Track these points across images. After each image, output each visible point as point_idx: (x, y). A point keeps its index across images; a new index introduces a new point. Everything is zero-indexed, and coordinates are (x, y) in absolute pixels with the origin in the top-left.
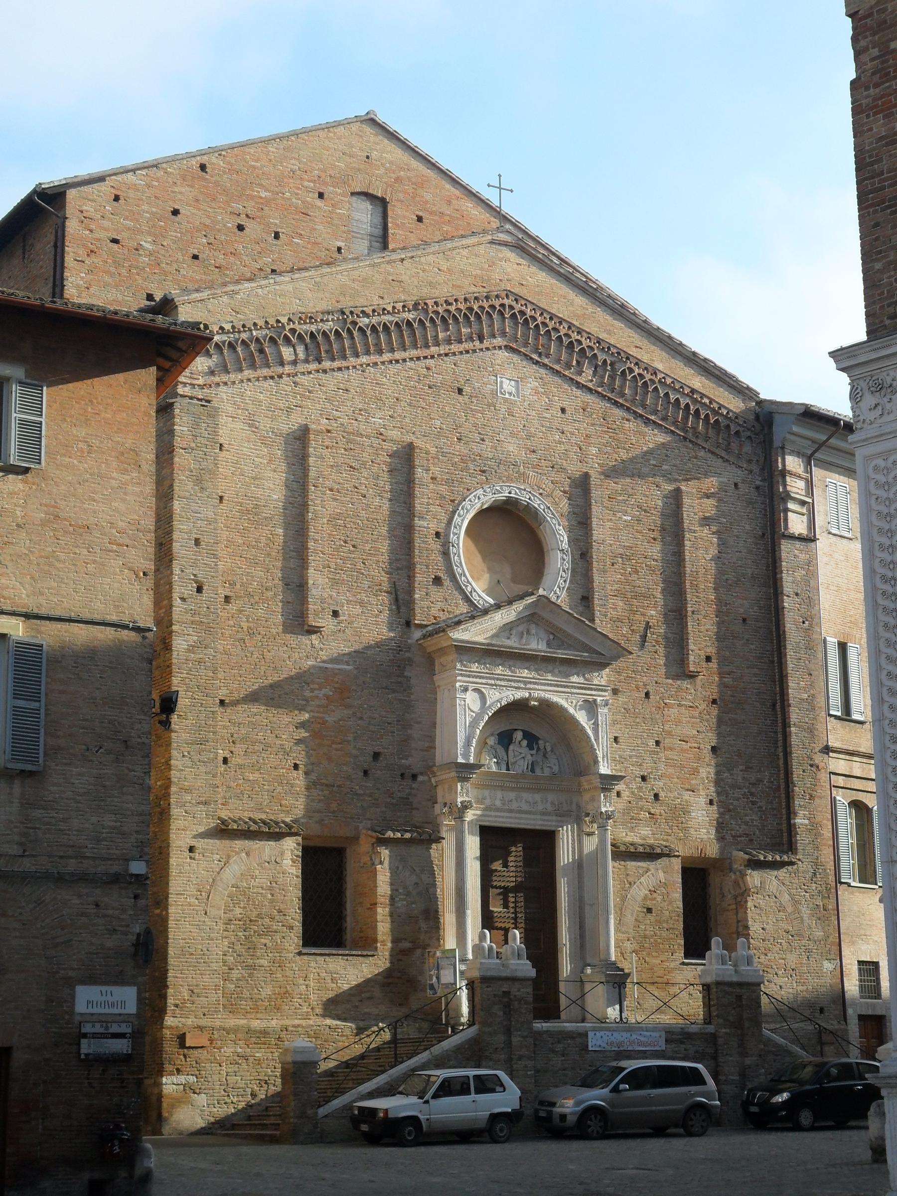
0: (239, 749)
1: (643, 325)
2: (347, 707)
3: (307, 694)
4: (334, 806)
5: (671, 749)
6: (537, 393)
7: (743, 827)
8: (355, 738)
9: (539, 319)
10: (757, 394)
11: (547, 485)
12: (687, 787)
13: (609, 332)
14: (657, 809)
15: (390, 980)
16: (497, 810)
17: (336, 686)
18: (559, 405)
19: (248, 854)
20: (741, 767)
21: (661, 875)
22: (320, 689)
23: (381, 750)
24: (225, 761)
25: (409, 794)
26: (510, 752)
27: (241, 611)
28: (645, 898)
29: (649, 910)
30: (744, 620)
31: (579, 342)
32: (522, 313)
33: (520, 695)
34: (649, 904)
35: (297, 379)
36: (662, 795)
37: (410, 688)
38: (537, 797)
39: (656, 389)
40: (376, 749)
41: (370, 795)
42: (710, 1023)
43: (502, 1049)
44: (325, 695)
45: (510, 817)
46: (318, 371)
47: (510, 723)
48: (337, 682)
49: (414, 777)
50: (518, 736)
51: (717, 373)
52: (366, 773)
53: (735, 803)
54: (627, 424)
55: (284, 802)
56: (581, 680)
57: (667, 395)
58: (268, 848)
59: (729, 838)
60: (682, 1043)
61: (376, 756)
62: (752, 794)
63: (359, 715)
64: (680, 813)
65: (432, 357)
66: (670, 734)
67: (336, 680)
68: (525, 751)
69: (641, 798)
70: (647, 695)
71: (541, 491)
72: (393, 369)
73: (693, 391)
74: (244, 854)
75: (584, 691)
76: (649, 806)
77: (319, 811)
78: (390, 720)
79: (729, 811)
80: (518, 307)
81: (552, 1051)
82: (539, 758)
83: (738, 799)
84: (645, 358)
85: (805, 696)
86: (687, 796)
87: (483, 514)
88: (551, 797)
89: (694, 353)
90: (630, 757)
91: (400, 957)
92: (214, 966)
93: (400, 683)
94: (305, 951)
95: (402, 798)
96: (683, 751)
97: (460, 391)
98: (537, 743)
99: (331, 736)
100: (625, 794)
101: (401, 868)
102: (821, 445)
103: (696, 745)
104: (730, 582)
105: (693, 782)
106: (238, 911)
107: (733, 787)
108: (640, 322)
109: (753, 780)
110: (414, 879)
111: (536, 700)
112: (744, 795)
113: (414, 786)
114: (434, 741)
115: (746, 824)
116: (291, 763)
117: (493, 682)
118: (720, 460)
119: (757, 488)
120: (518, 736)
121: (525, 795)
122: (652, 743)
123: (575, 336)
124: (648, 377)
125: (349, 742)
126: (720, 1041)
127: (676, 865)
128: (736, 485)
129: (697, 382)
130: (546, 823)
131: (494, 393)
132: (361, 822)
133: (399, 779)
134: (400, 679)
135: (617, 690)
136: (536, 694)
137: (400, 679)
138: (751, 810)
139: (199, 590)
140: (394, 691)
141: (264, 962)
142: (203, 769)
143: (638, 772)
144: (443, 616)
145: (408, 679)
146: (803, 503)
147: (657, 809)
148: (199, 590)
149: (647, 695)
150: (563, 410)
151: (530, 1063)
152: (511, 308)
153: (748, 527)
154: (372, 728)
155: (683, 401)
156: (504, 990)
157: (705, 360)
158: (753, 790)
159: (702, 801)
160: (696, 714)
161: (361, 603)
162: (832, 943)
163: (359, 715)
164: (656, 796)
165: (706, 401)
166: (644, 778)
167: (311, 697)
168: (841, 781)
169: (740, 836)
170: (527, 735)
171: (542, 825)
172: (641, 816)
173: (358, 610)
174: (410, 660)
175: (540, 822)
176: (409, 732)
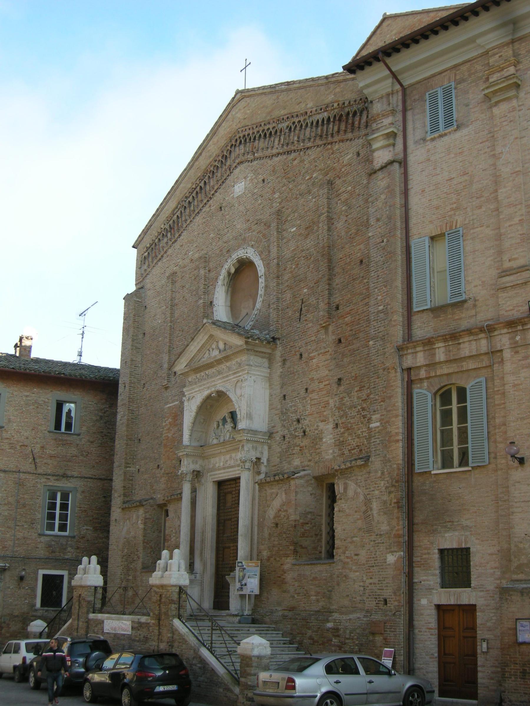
7: (357, 440)
12: (322, 418)
20: (356, 389)
28: (274, 518)
33: (206, 393)
53: (352, 421)
66: (312, 379)
76: (297, 441)
79: (348, 429)
85: (381, 308)
96: (321, 390)
105: (325, 413)
138: (362, 423)
147: (305, 442)
158: (365, 405)
159: (331, 426)
169: (354, 449)
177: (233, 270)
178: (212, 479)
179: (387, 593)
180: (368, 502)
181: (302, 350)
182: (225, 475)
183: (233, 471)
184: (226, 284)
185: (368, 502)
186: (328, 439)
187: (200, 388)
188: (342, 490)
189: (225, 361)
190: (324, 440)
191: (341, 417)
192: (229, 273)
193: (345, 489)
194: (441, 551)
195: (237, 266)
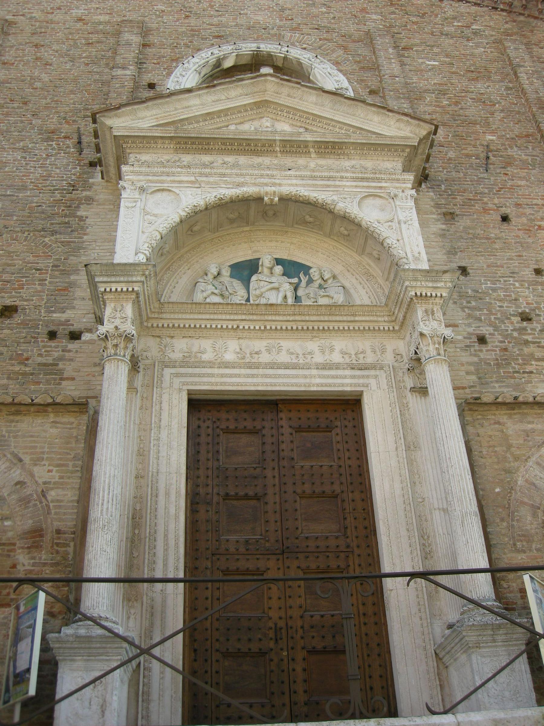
25: (61, 359)
38: (313, 345)
45: (253, 376)
69: (527, 342)
71: (305, 46)
75: (365, 184)
88: (340, 344)
90: (494, 290)
95: (45, 365)
98: (306, 273)
100: (495, 341)
113: (71, 346)
121: (286, 344)
137: (67, 220)
140: (54, 233)
166: (526, 318)
171: (318, 385)
175: (318, 381)
176: (72, 277)
177: (228, 63)
182: (250, 380)
183: (305, 377)
184: (202, 75)
189: (317, 153)
192: (219, 63)
195: (243, 62)
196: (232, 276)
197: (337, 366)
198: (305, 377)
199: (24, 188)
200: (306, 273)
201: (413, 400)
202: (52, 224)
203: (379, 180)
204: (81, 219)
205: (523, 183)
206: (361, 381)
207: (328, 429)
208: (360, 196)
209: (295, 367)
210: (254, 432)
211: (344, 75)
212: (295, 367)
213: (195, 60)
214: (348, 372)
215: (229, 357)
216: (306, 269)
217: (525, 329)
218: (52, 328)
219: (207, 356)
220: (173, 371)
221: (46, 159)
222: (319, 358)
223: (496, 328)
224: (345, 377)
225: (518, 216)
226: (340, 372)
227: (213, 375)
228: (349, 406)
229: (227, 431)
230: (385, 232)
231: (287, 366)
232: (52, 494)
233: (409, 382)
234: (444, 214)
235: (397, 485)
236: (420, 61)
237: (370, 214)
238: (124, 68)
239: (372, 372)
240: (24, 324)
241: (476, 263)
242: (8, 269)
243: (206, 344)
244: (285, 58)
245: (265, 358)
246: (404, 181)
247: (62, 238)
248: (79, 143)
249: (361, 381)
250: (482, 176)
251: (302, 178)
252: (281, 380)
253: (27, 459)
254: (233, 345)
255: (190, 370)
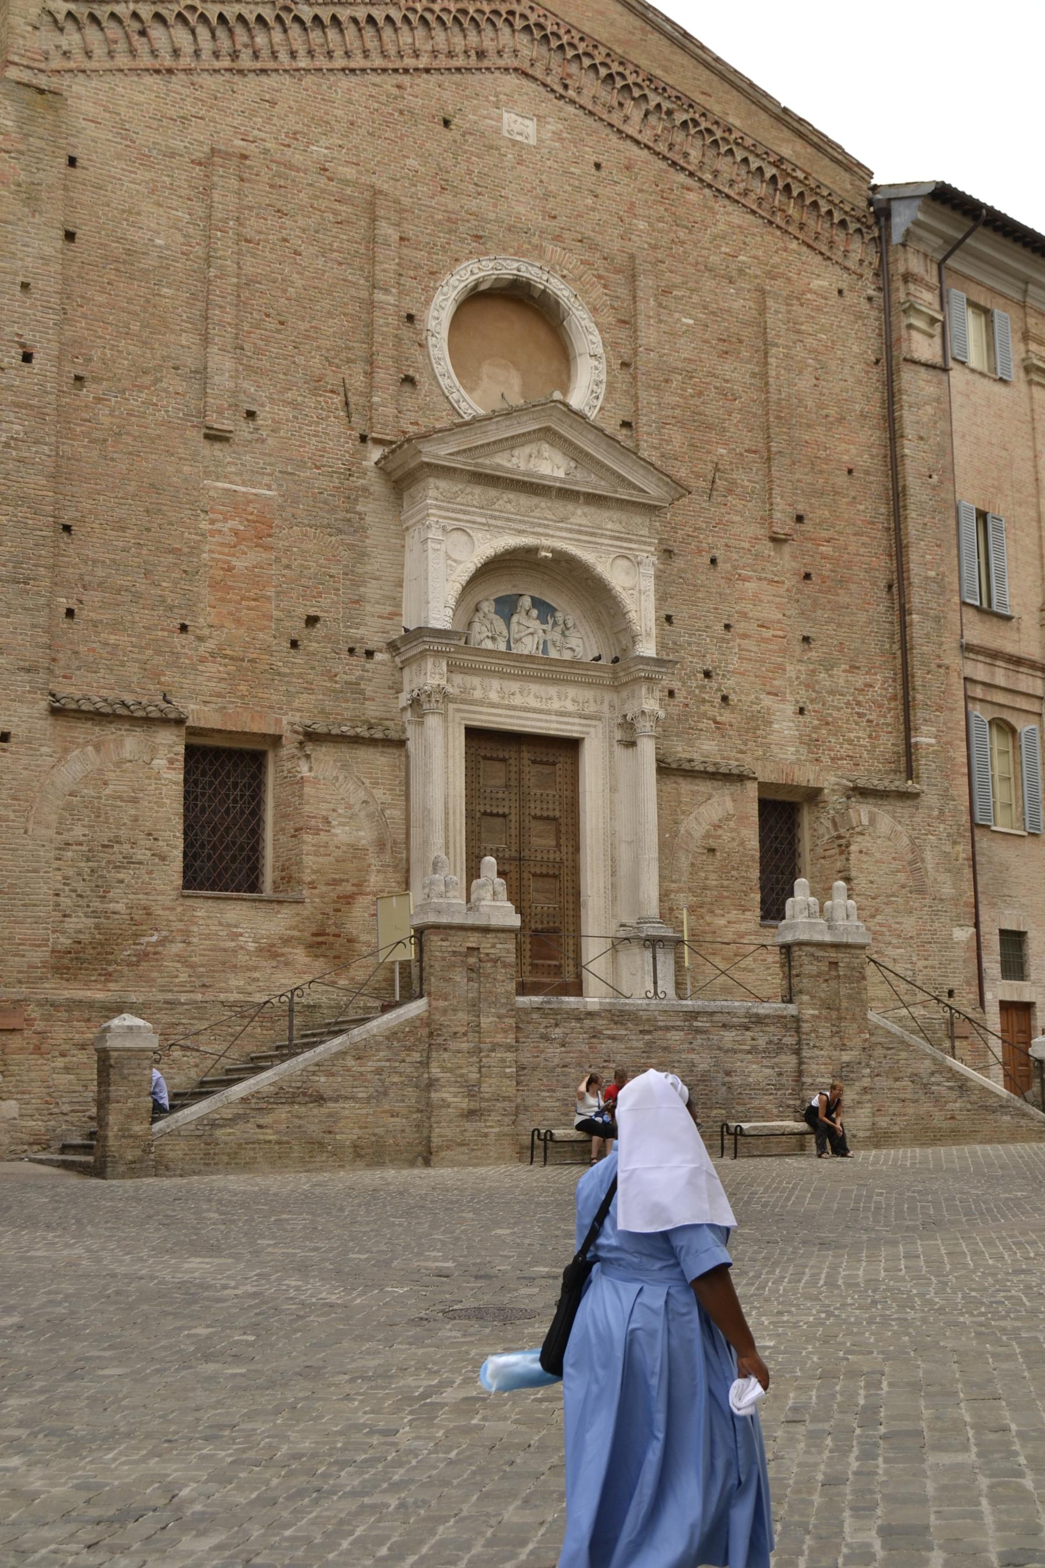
0: (94, 597)
1: (713, 63)
2: (268, 548)
3: (204, 525)
4: (243, 688)
5: (745, 636)
6: (561, 139)
8: (278, 593)
9: (565, 39)
10: (871, 174)
11: (572, 260)
12: (768, 688)
13: (666, 70)
14: (726, 717)
15: (320, 939)
16: (493, 705)
17: (250, 517)
18: (594, 158)
19: (97, 748)
21: (729, 805)
22: (225, 520)
23: (318, 614)
24: (70, 613)
25: (362, 678)
26: (514, 626)
27: (98, 400)
28: (707, 836)
29: (712, 851)
30: (850, 471)
31: (623, 76)
32: (540, 26)
34: (712, 843)
35: (195, 78)
36: (733, 697)
37: (364, 529)
39: (730, 152)
40: (312, 612)
41: (300, 676)
42: (790, 1001)
43: (465, 1034)
44: (231, 530)
45: (511, 717)
46: (230, 70)
47: (514, 586)
48: (252, 514)
49: (369, 654)
50: (526, 602)
51: (815, 139)
52: (294, 644)
53: (835, 714)
54: (692, 196)
55: (163, 679)
56: (617, 527)
57: (745, 160)
58: (131, 743)
59: (826, 760)
60: (748, 1029)
61: (312, 621)
62: (859, 703)
63: (284, 561)
64: (757, 723)
65: (406, 71)
66: (744, 615)
67: (250, 509)
68: (535, 625)
69: (704, 701)
70: (713, 561)
71: (565, 272)
72: (345, 82)
73: (782, 160)
74: (90, 748)
75: (619, 543)
77: (219, 695)
78: (332, 572)
79: (827, 724)
80: (533, 18)
81: (546, 1038)
82: (556, 636)
83: (839, 709)
84: (717, 109)
85: (932, 574)
86: (767, 701)
87: (476, 298)
88: (572, 692)
89: (785, 110)
90: (689, 644)
91: (338, 906)
92: (41, 912)
93: (349, 520)
94: (187, 892)
95: (350, 683)
97: (446, 123)
98: (553, 616)
99: (241, 589)
100: (680, 696)
101: (341, 778)
102: (955, 247)
103: (781, 633)
104: (831, 419)
105: (776, 683)
106: (78, 831)
107: (831, 692)
108: (709, 59)
109: (859, 684)
110: (362, 795)
111: (548, 549)
112: (848, 703)
113: (368, 666)
114: (400, 606)
115: (850, 742)
116: (177, 623)
117: (484, 520)
118: (820, 257)
119: (870, 299)
120: (526, 602)
122: (719, 628)
123: (615, 67)
124: (719, 134)
125: (268, 599)
126: (806, 1027)
127: (752, 790)
128: (840, 292)
129: (789, 148)
130: (563, 727)
131: (497, 131)
132: (286, 714)
133: (345, 655)
134: (348, 516)
135: (670, 551)
136: (546, 542)
137: (348, 516)
138: (857, 724)
139: (27, 358)
140: (340, 531)
141: (120, 907)
142: (28, 621)
143: (699, 667)
144: (412, 429)
145: (361, 516)
146: (933, 321)
147: (726, 717)
148: (27, 358)
149: (713, 561)
150: (598, 166)
151: (510, 1056)
152: (523, 16)
153: (855, 349)
154: (304, 581)
155: (770, 171)
156: (470, 945)
157: (800, 120)
158: (861, 698)
159: (790, 709)
160: (782, 591)
161: (293, 404)
162: (966, 904)
163: (284, 561)
164: (725, 699)
165: (800, 175)
166: (707, 674)
167: (210, 531)
168: (978, 692)
169: (842, 759)
170: (536, 603)
172: (701, 726)
173: (288, 412)
174: (365, 489)
175: (555, 726)
176: (362, 589)
177: (483, 287)
178: (463, 719)
179: (954, 982)
180: (916, 847)
181: (717, 553)
183: (547, 721)
185: (916, 847)
186: (785, 725)
187: (491, 521)
188: (865, 821)
190: (776, 726)
191: (812, 701)
193: (872, 821)
194: (1003, 932)
196: (496, 613)
197: (569, 714)
198: (547, 721)
199: (302, 465)
200: (553, 616)
201: (618, 750)
202: (336, 520)
203: (630, 541)
204: (361, 516)
205: (737, 518)
206: (585, 729)
207: (554, 764)
208: (613, 556)
209: (540, 711)
210: (504, 760)
211: (600, 331)
212: (540, 711)
213: (453, 281)
214: (577, 720)
215: (494, 696)
216: (553, 610)
217: (704, 687)
218: (351, 645)
219: (478, 694)
220: (455, 706)
221: (318, 423)
222: (556, 705)
223: (684, 683)
224: (574, 724)
225: (725, 562)
226: (571, 720)
227: (481, 713)
228: (571, 746)
229: (485, 758)
230: (629, 603)
231: (535, 711)
232: (388, 812)
233: (618, 735)
234: (665, 551)
235: (601, 820)
236: (677, 315)
237: (617, 576)
238: (386, 291)
239: (593, 722)
240: (328, 638)
241: (681, 614)
242: (305, 572)
243: (476, 681)
244: (544, 292)
245: (518, 701)
246: (650, 544)
247: (349, 539)
248: (347, 404)
249: (585, 729)
250: (704, 505)
251: (571, 531)
252: (529, 723)
253: (367, 782)
254: (496, 684)
255: (467, 707)
